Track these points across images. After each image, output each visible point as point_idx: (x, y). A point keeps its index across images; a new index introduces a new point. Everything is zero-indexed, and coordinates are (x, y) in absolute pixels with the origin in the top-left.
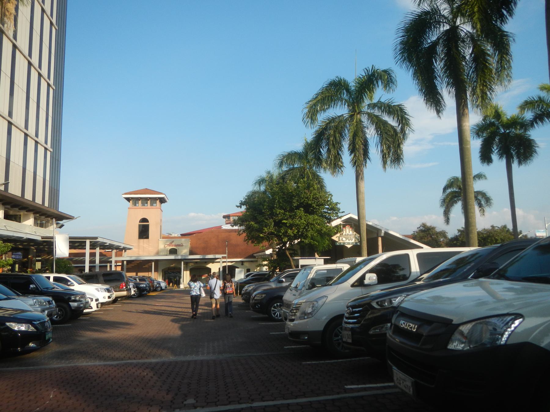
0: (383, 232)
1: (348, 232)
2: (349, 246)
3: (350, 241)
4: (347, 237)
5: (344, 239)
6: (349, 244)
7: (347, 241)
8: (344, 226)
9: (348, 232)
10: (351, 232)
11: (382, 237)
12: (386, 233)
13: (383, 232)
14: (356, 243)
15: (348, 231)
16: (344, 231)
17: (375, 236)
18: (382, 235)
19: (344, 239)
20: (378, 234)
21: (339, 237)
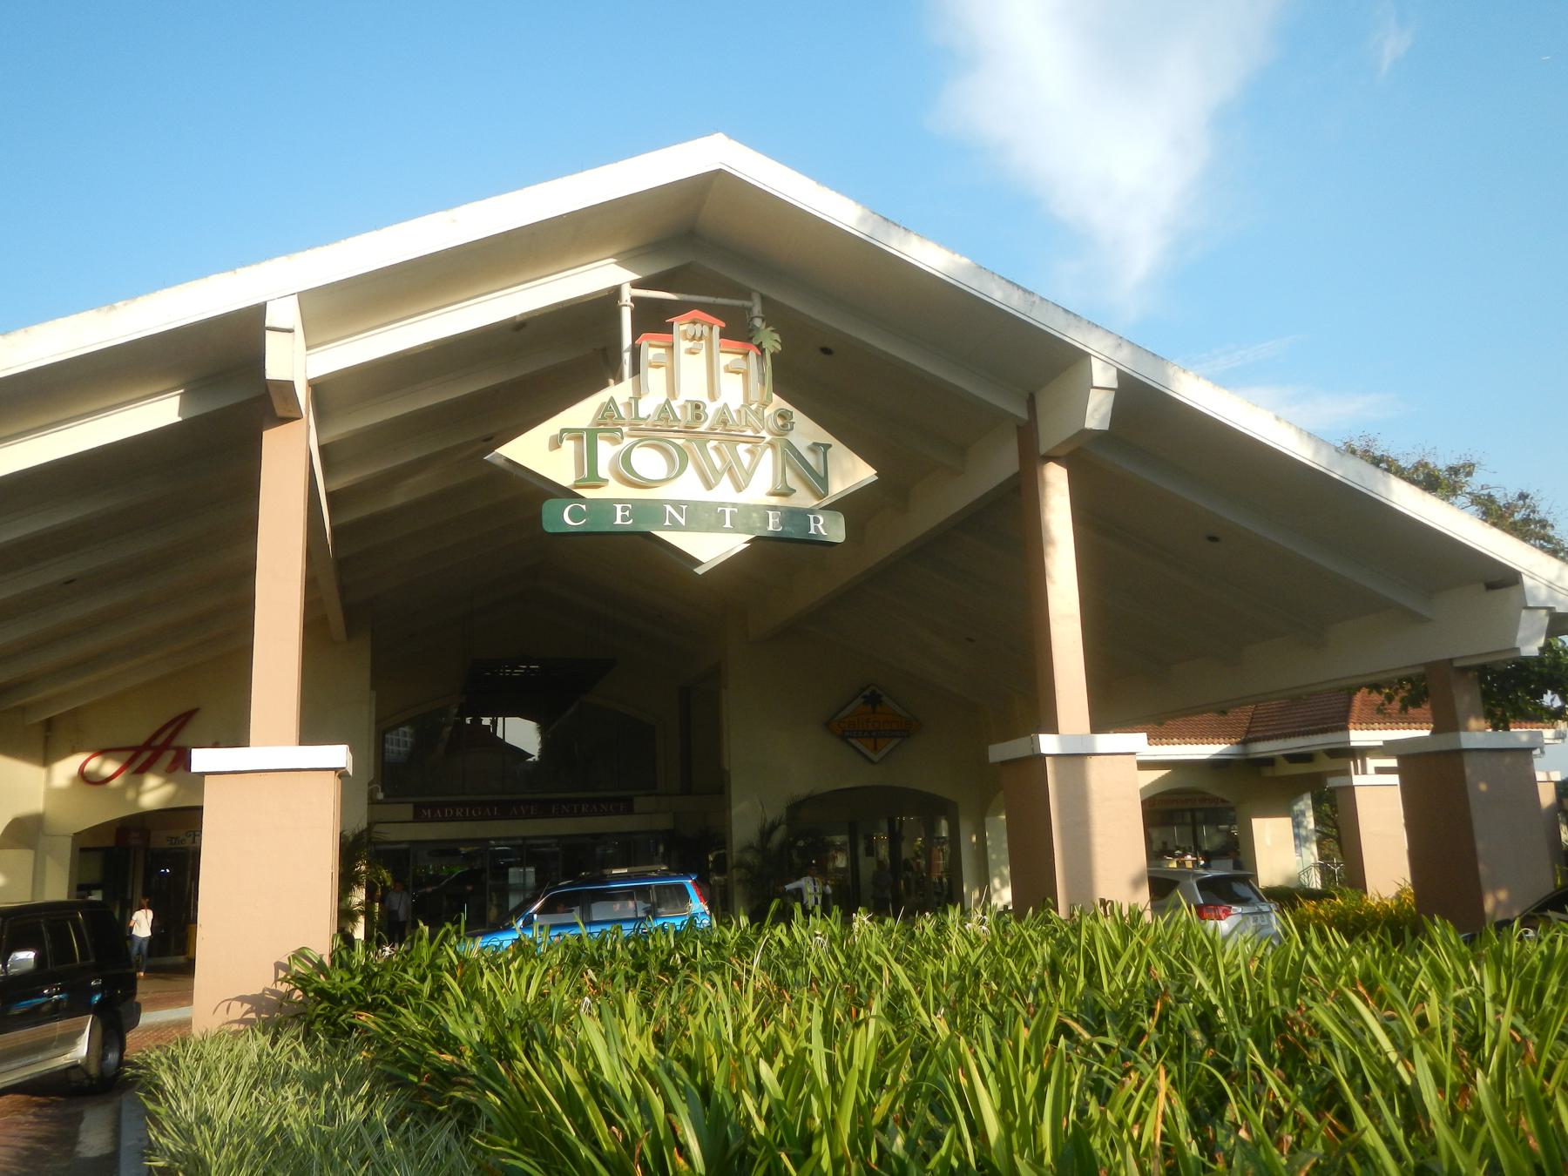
0: (1103, 375)
1: (692, 384)
2: (710, 548)
3: (724, 492)
4: (679, 432)
5: (648, 462)
6: (702, 517)
7: (688, 487)
8: (653, 319)
9: (692, 384)
10: (732, 392)
11: (1083, 457)
12: (1140, 403)
13: (1103, 375)
14: (797, 516)
15: (700, 374)
16: (655, 378)
17: (1006, 464)
18: (1097, 413)
19: (648, 462)
20: (1027, 434)
21: (587, 439)
